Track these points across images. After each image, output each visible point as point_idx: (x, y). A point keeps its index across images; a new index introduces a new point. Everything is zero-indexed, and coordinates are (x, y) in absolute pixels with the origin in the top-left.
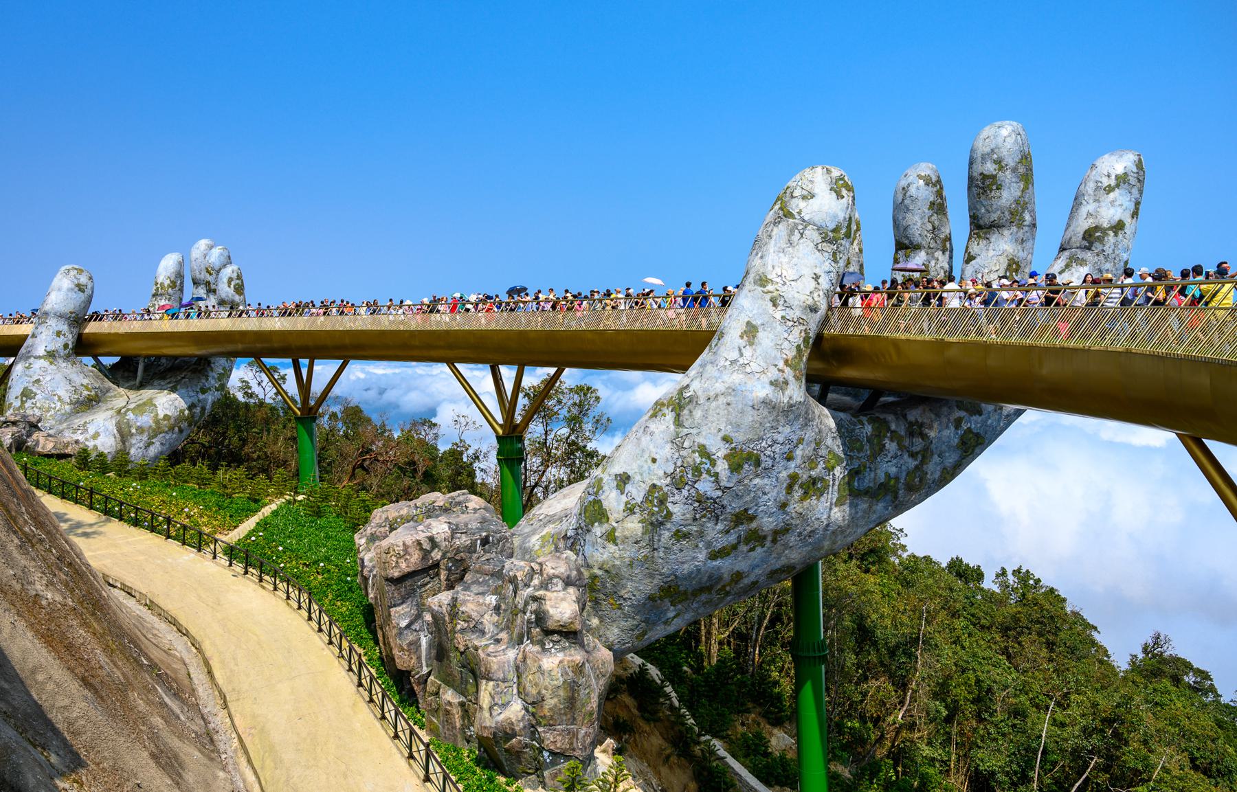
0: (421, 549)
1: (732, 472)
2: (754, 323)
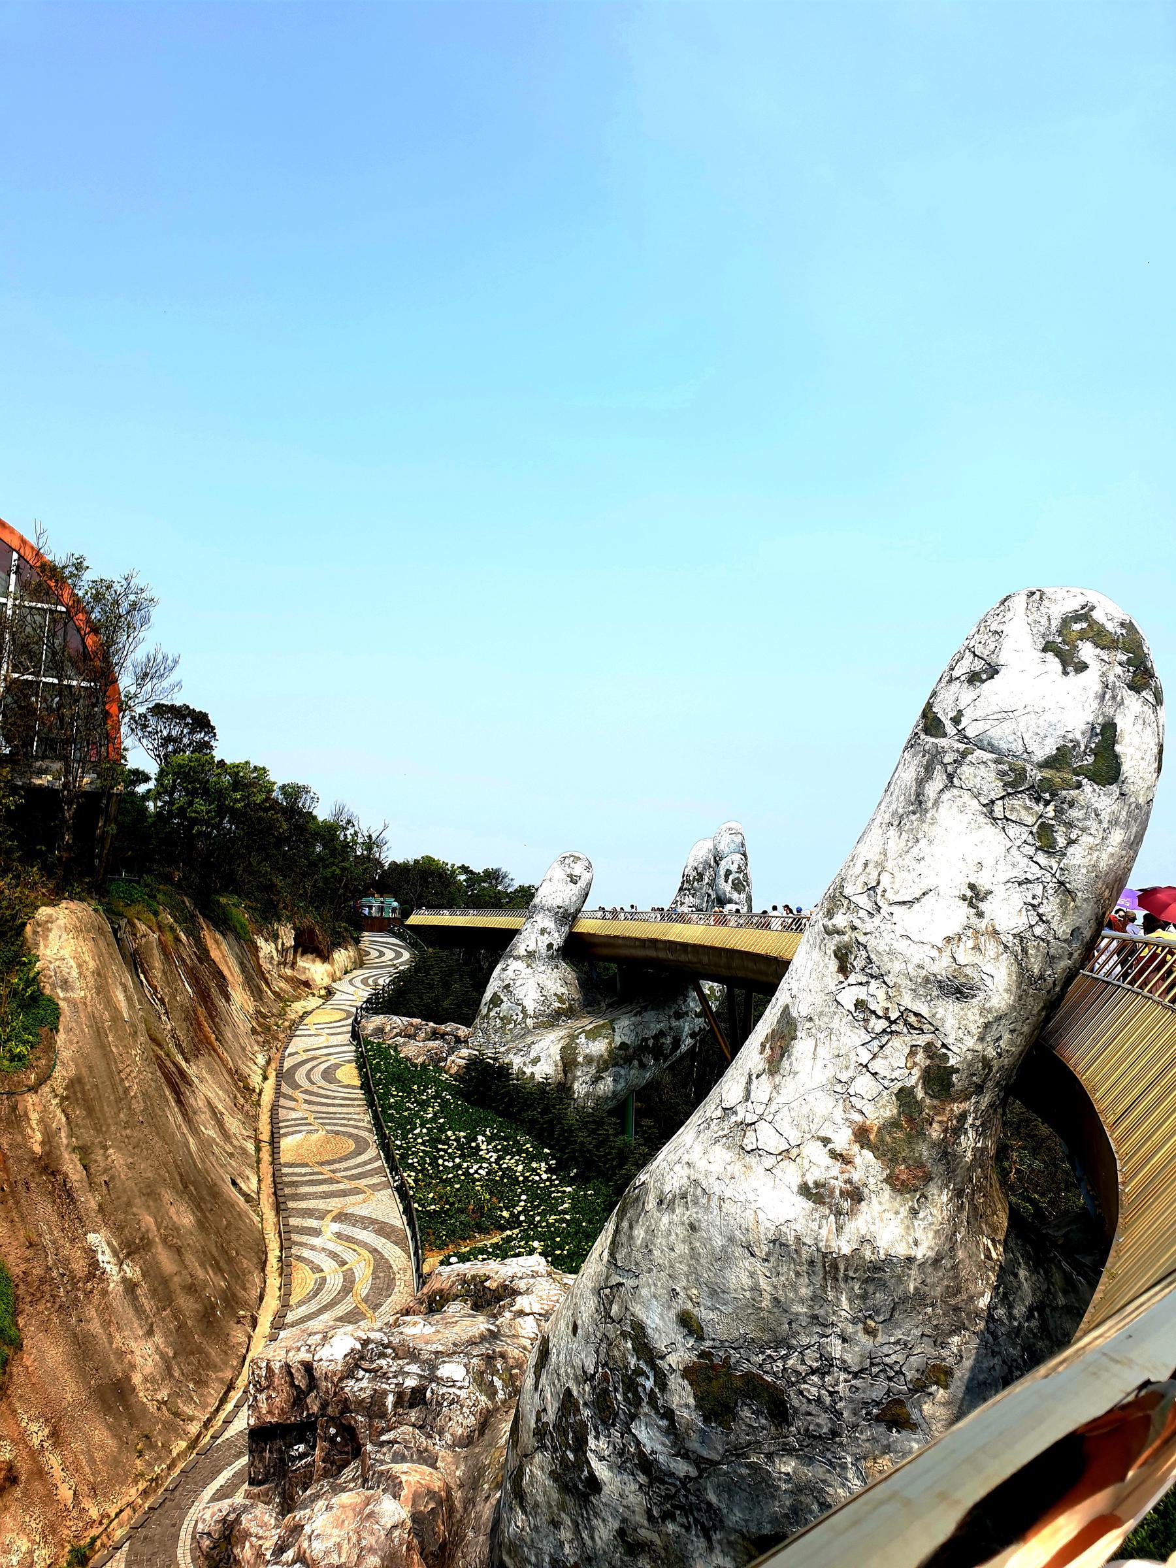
0: (292, 1384)
1: (706, 1420)
2: (794, 1014)
